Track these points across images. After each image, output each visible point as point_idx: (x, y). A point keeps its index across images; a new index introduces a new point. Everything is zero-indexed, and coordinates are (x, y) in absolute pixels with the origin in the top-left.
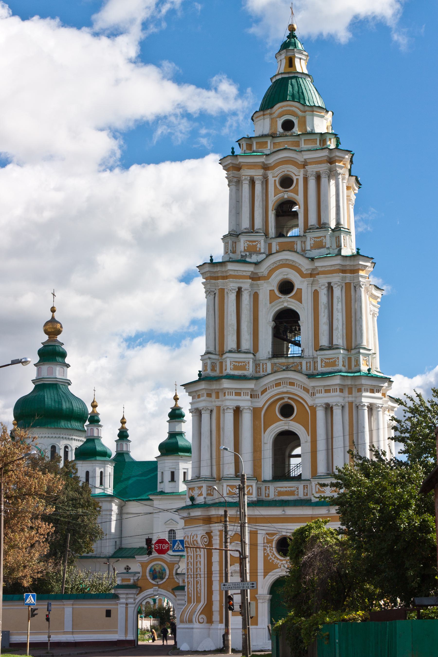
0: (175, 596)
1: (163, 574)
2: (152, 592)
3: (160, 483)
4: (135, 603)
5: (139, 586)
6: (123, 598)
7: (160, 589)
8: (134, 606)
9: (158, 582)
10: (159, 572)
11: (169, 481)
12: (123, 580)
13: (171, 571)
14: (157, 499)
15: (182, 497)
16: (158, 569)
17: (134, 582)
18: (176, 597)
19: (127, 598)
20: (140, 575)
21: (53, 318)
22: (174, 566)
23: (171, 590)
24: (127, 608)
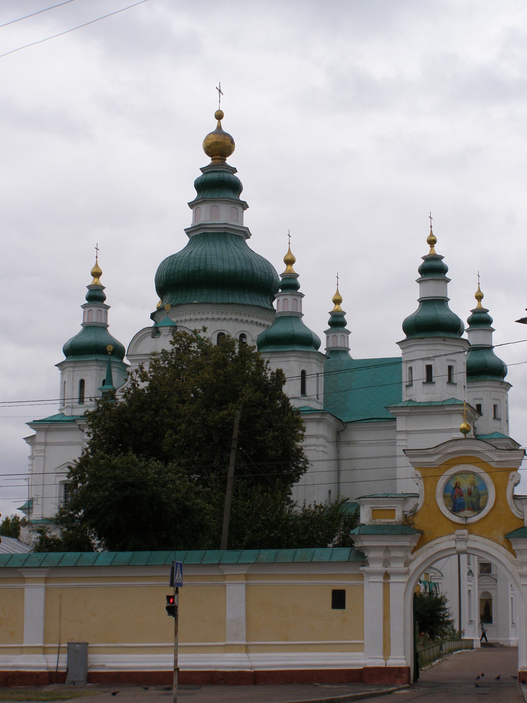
0: (513, 553)
1: (479, 499)
2: (453, 544)
3: (407, 386)
4: (407, 573)
5: (417, 527)
6: (377, 560)
7: (472, 537)
8: (404, 579)
9: (466, 518)
10: (470, 493)
11: (423, 383)
12: (375, 512)
13: (500, 489)
14: (401, 414)
15: (447, 409)
16: (465, 485)
17: (405, 516)
18: (515, 556)
19: (386, 562)
20: (420, 501)
21: (219, 127)
22: (508, 476)
23: (501, 539)
24: (386, 586)
